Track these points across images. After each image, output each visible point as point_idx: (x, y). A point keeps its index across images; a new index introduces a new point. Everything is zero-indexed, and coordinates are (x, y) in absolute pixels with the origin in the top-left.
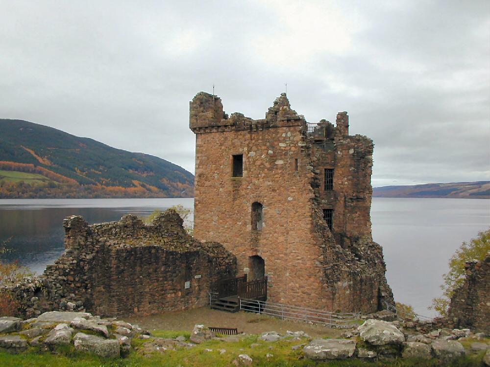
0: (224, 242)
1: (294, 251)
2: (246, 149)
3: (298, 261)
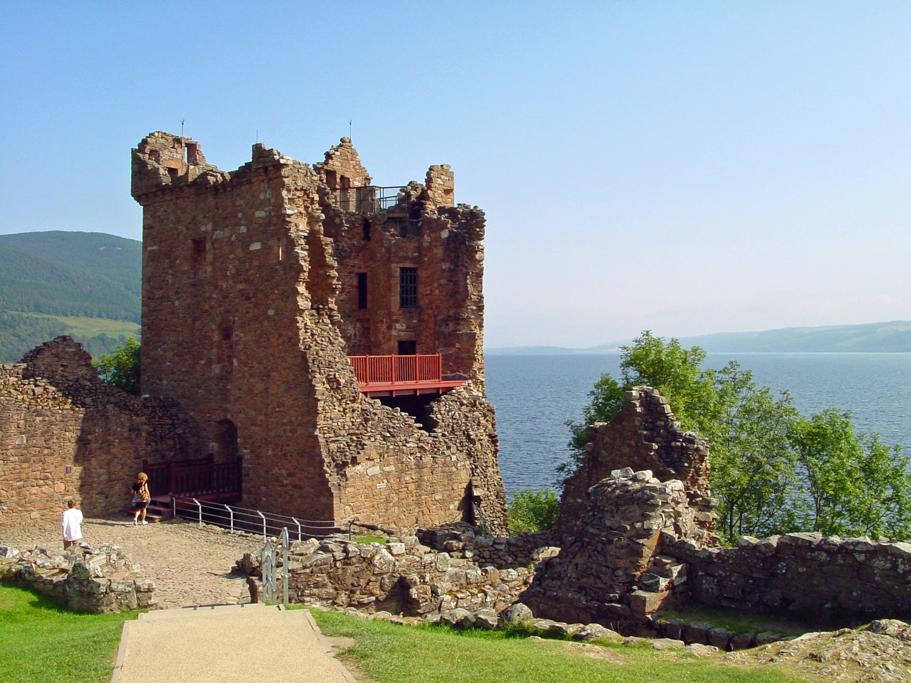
2: (209, 227)
3: (285, 427)
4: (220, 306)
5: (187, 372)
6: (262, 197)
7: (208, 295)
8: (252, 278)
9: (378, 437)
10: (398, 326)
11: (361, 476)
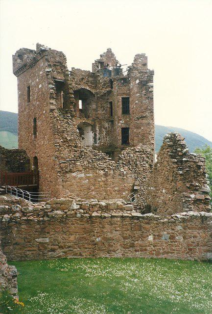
10: (121, 122)
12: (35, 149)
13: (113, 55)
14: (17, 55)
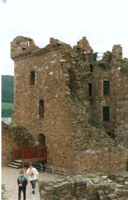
0: (27, 126)
1: (59, 130)
2: (36, 67)
3: (62, 136)
4: (40, 94)
5: (29, 117)
6: (53, 56)
7: (35, 91)
8: (50, 84)
9: (94, 140)
10: (103, 101)
11: (89, 154)
12: (41, 127)
13: (87, 42)
14: (15, 42)
